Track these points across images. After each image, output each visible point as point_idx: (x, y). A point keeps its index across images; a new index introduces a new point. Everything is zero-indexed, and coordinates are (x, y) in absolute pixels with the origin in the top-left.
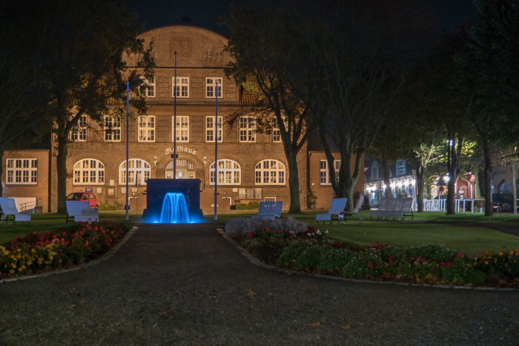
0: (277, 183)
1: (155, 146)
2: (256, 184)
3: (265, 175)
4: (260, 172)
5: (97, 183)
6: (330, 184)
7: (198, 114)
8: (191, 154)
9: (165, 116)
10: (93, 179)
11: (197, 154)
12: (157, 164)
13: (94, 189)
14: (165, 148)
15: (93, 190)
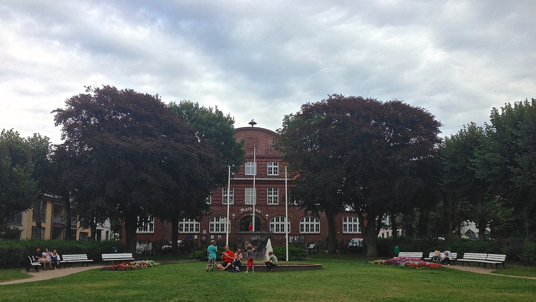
0: (315, 232)
2: (301, 232)
5: (194, 232)
10: (192, 230)
13: (192, 236)
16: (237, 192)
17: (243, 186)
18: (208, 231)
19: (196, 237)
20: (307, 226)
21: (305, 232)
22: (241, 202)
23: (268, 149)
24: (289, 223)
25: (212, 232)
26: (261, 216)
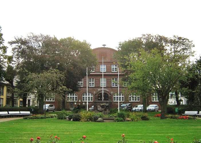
0: (137, 101)
1: (95, 88)
2: (130, 101)
5: (75, 101)
6: (158, 101)
16: (96, 80)
18: (81, 100)
19: (75, 103)
23: (112, 58)
25: (84, 101)
26: (109, 93)
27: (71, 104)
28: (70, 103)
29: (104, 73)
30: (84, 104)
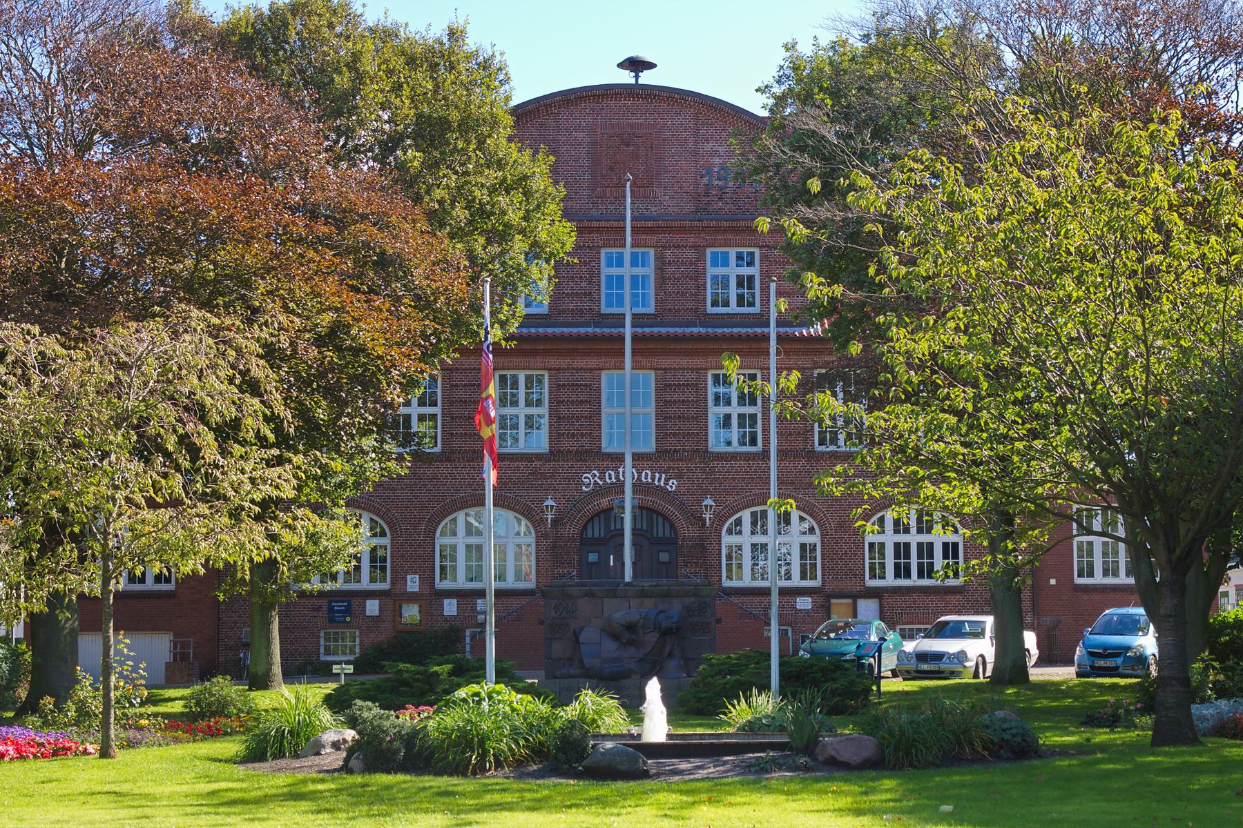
1: (548, 466)
3: (897, 556)
4: (882, 545)
5: (365, 584)
6: (1131, 581)
7: (684, 362)
8: (662, 489)
9: (577, 370)
11: (683, 489)
12: (554, 522)
14: (579, 474)
15: (355, 607)
17: (592, 362)
18: (427, 579)
19: (372, 607)
20: (902, 550)
21: (890, 580)
22: (586, 440)
23: (708, 187)
24: (815, 539)
27: (331, 609)
28: (324, 603)
29: (615, 331)
30: (450, 607)
